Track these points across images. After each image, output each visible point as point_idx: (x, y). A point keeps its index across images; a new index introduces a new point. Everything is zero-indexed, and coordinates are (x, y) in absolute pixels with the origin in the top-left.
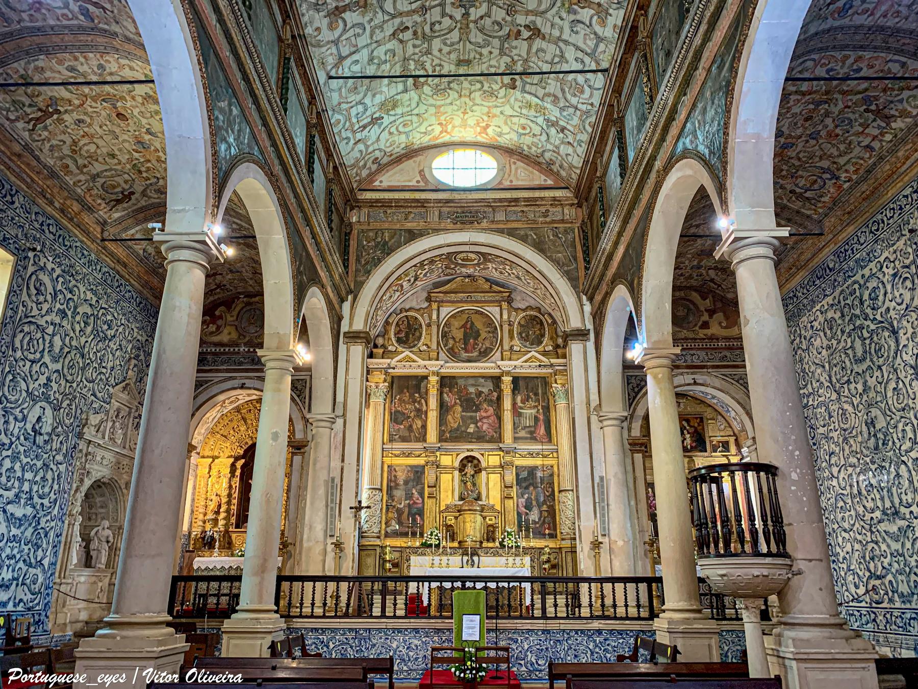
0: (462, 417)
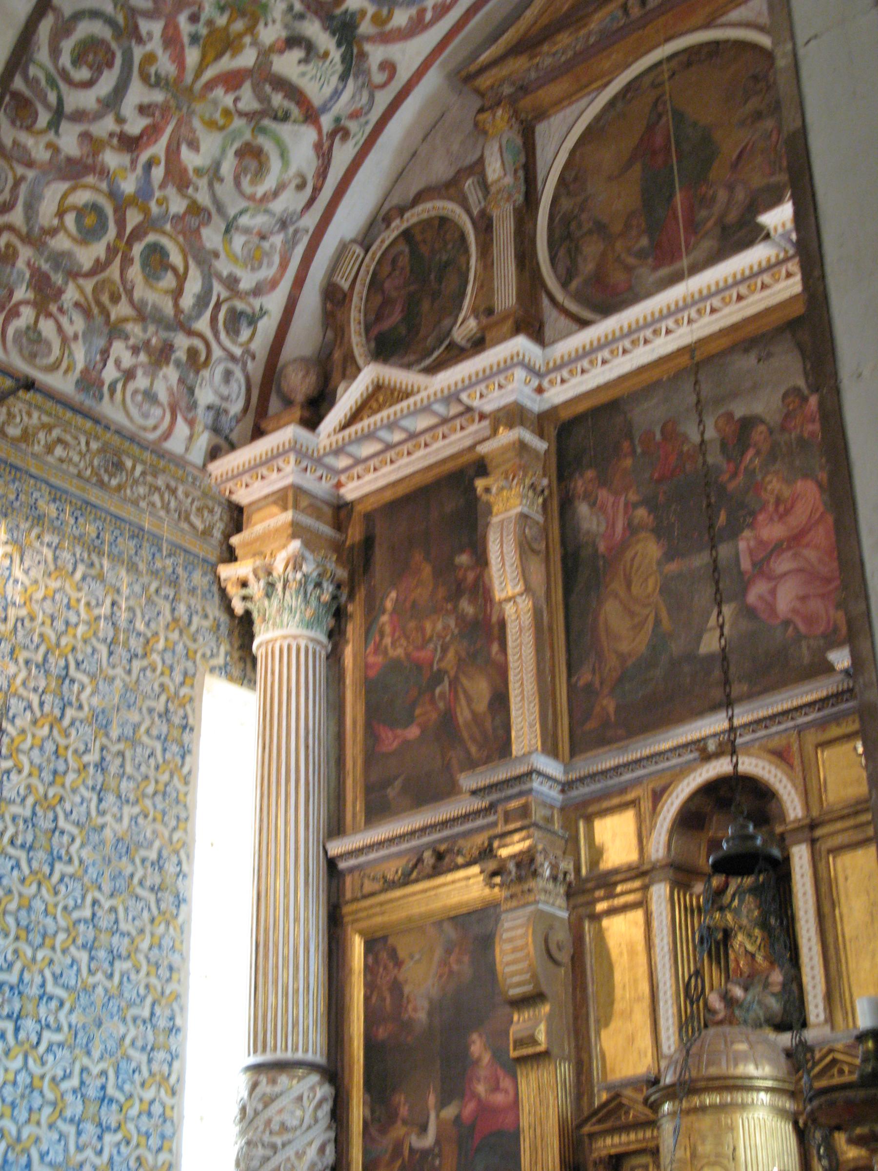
0: (664, 590)
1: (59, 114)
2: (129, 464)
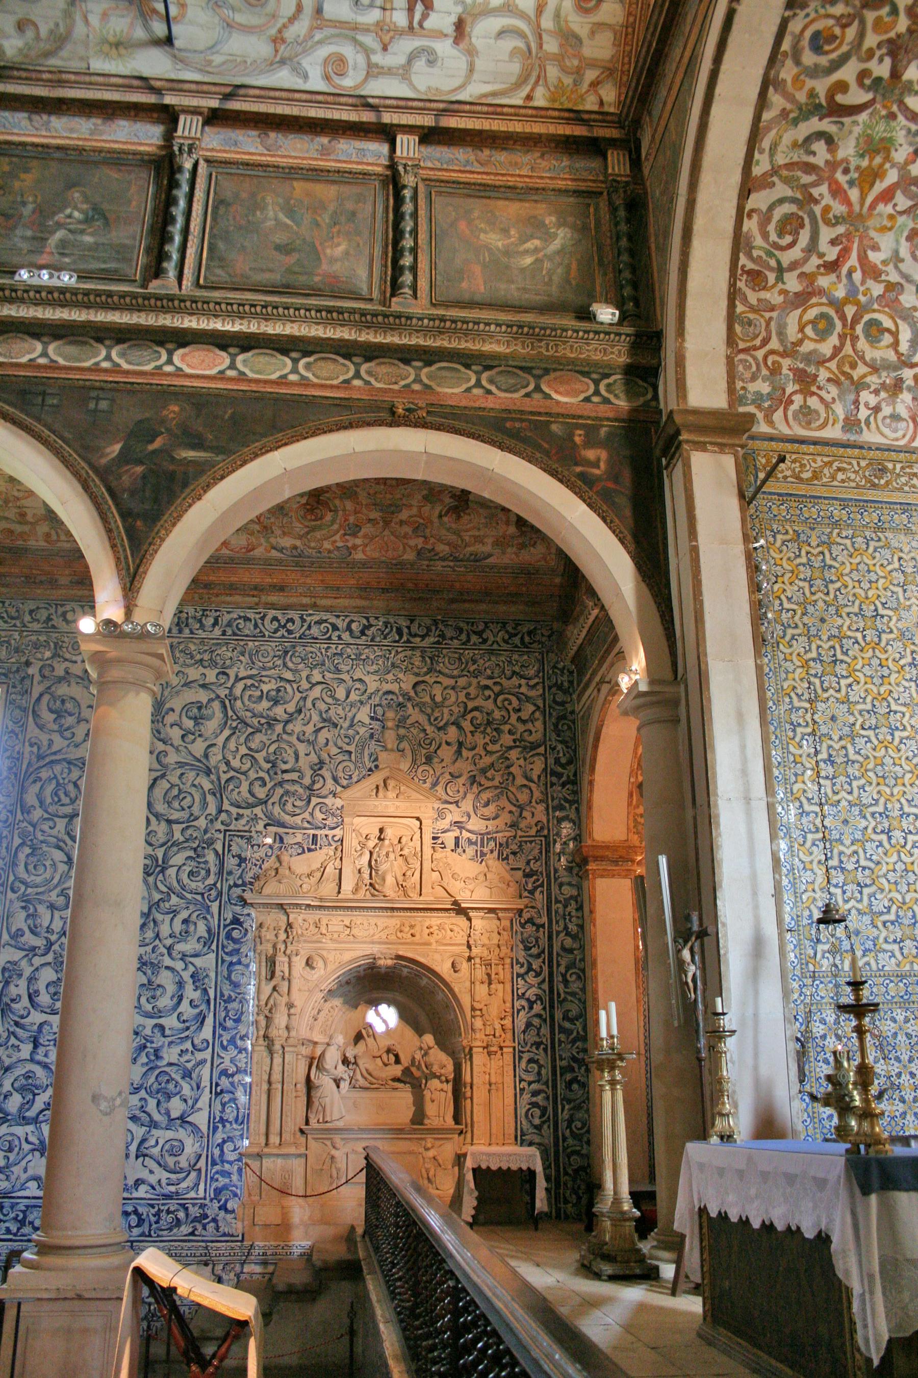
1: (780, 270)
2: (890, 466)
